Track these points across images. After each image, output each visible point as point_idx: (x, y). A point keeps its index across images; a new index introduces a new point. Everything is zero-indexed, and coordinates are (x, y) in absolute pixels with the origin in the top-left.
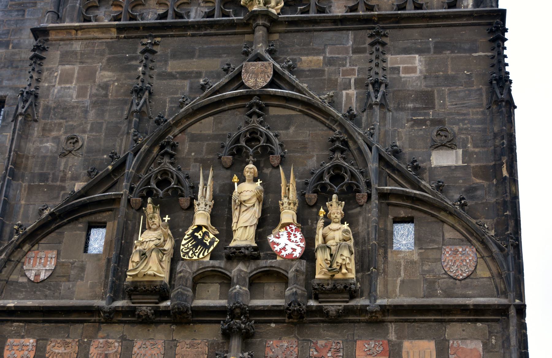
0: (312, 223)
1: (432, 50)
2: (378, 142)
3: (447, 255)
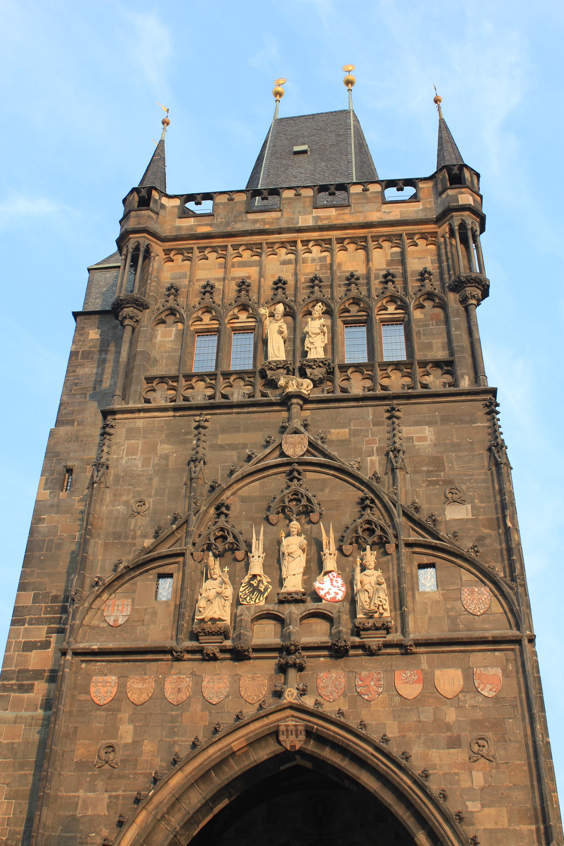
1: (439, 422)
3: (466, 595)
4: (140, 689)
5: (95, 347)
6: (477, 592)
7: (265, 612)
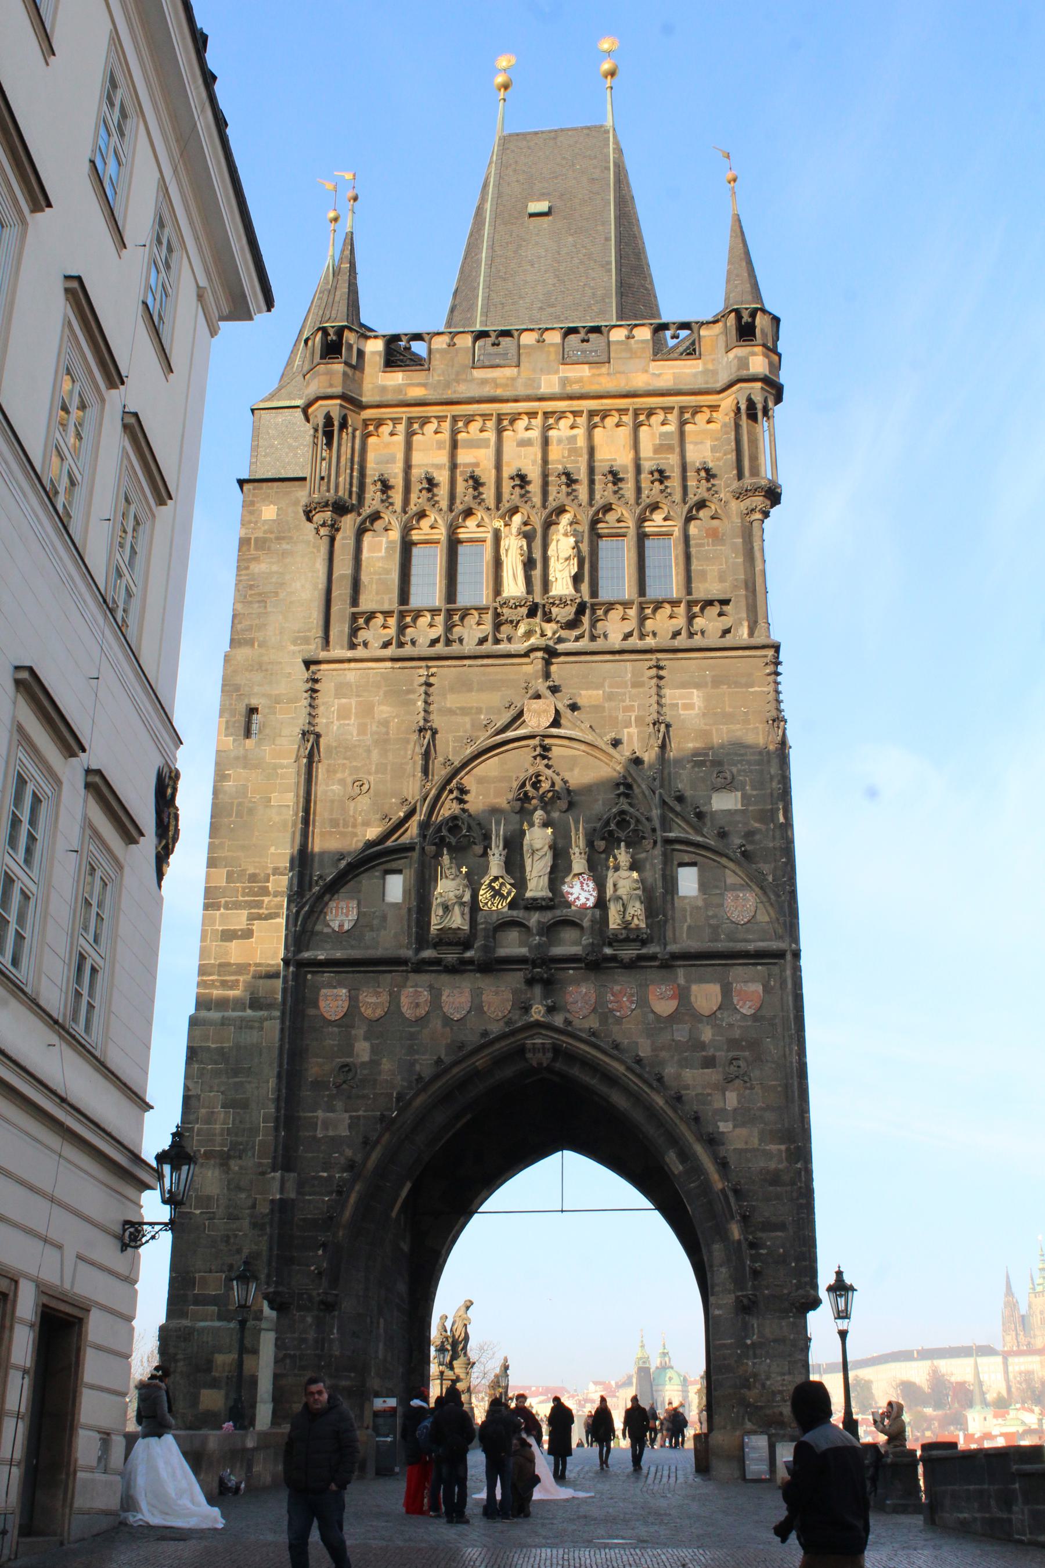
1: (710, 684)
2: (662, 786)
4: (374, 1004)
5: (272, 533)
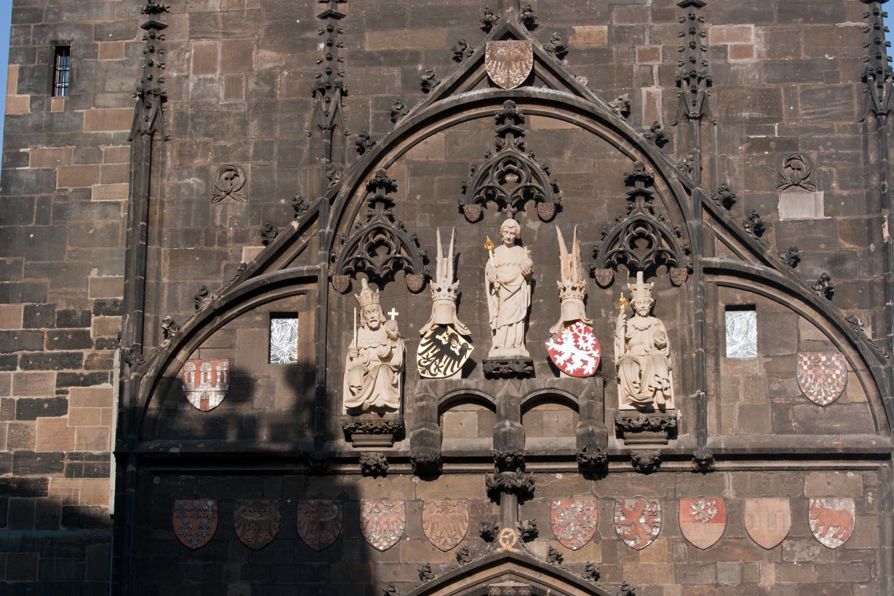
0: (607, 314)
1: (775, 15)
3: (805, 367)
4: (256, 523)
6: (824, 364)
7: (462, 392)
